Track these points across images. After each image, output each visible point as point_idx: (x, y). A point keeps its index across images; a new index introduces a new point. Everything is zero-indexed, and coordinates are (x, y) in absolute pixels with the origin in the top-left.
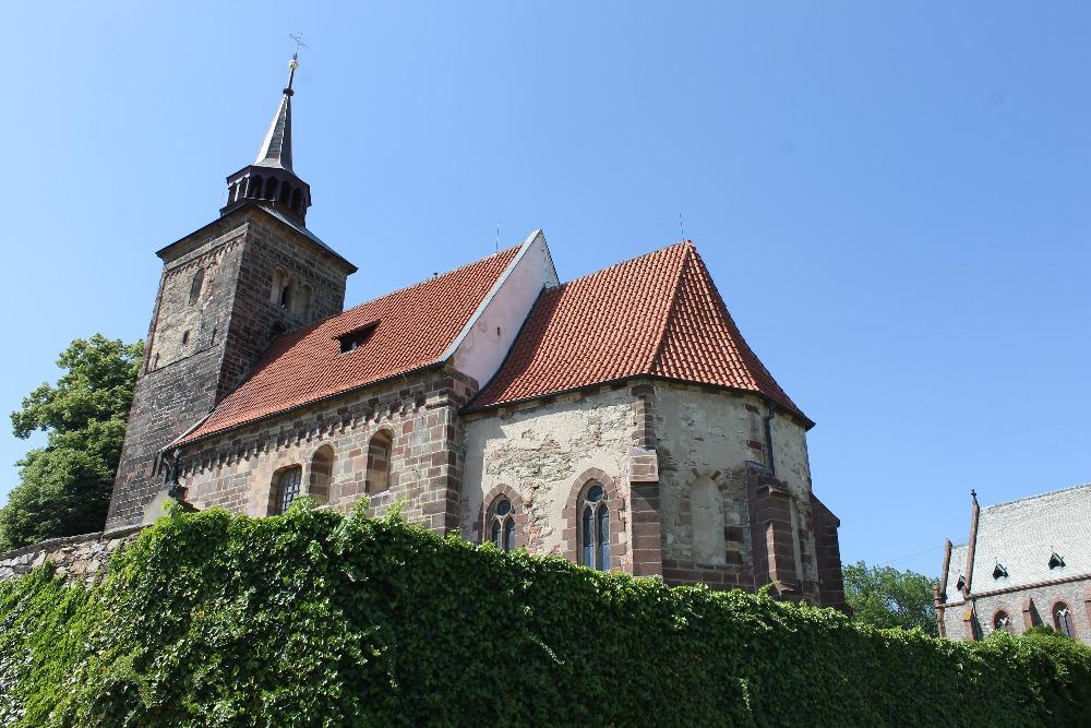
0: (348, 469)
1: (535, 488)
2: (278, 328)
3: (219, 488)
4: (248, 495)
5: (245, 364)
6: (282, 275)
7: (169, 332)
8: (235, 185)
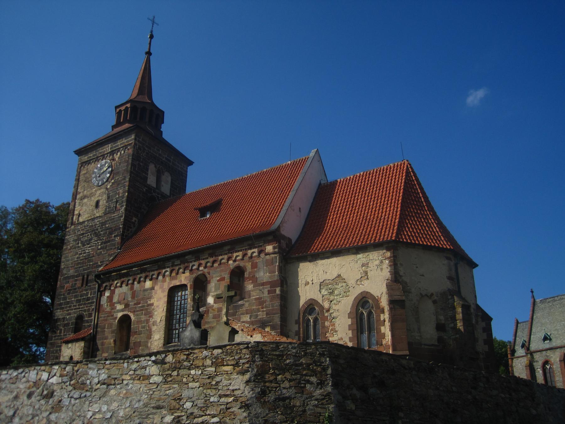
8: (120, 111)
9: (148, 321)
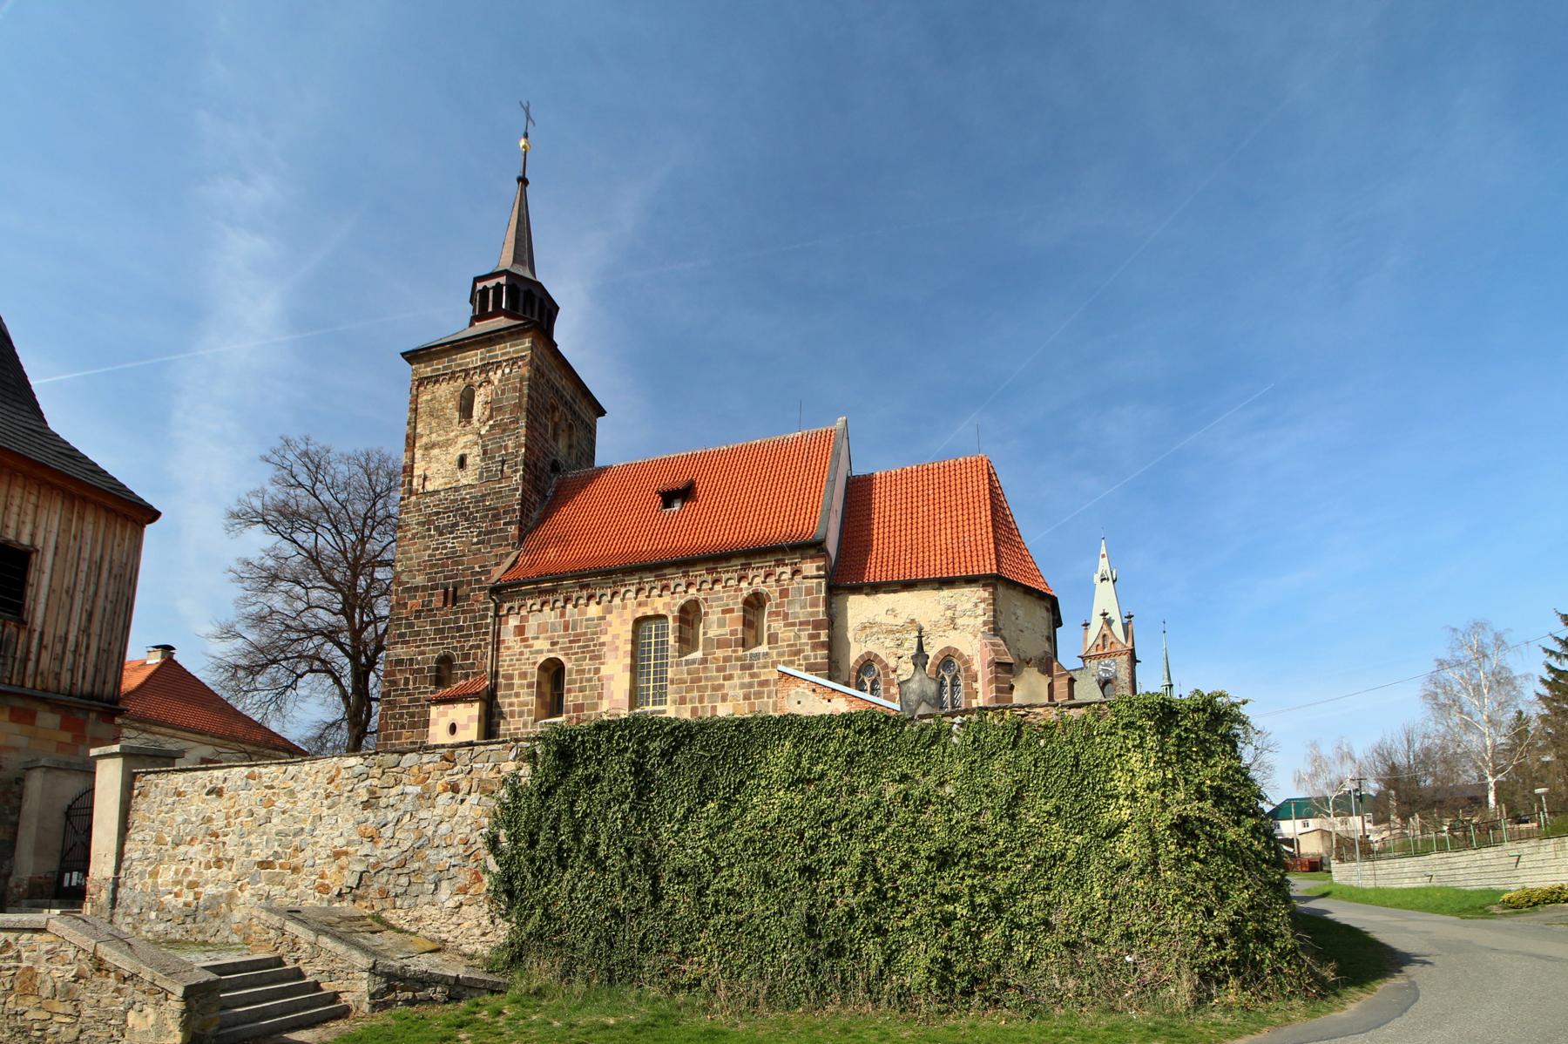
0: (721, 624)
3: (566, 628)
9: (597, 671)
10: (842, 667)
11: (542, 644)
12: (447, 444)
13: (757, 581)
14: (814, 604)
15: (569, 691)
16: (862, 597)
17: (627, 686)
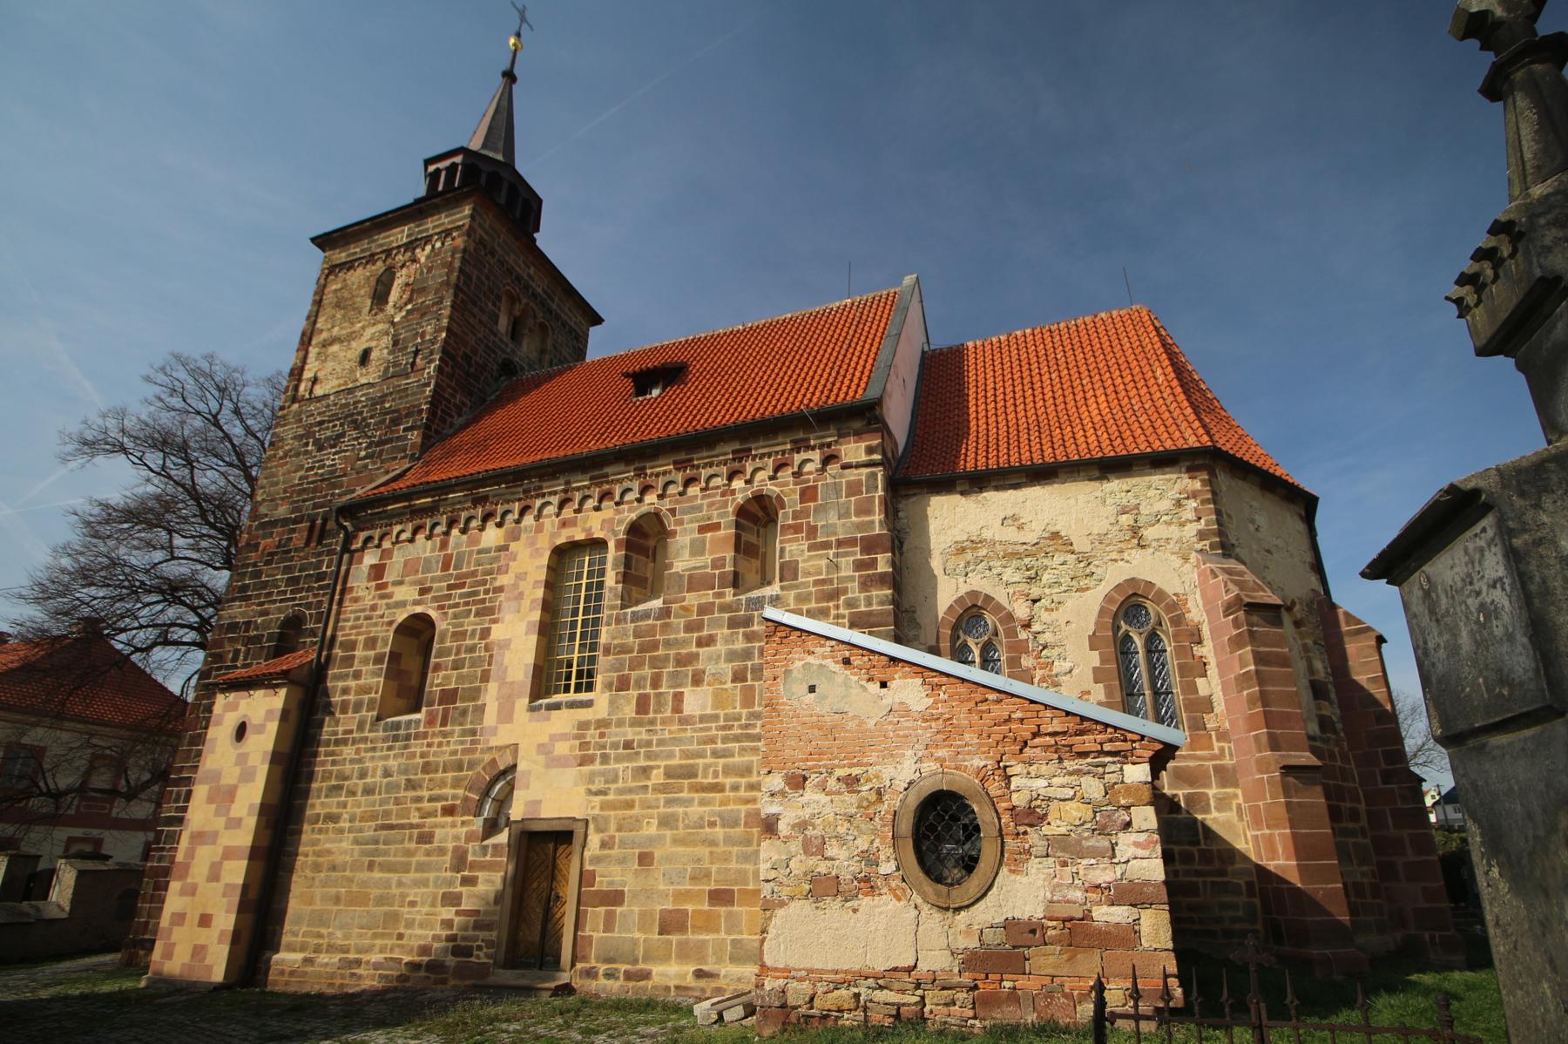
0: (697, 549)
1: (1035, 601)
2: (508, 368)
3: (446, 567)
4: (503, 580)
5: (464, 404)
6: (513, 299)
7: (335, 348)
9: (486, 633)
10: (923, 617)
11: (406, 593)
12: (351, 337)
13: (761, 476)
14: (864, 509)
15: (438, 667)
16: (955, 499)
17: (530, 658)
